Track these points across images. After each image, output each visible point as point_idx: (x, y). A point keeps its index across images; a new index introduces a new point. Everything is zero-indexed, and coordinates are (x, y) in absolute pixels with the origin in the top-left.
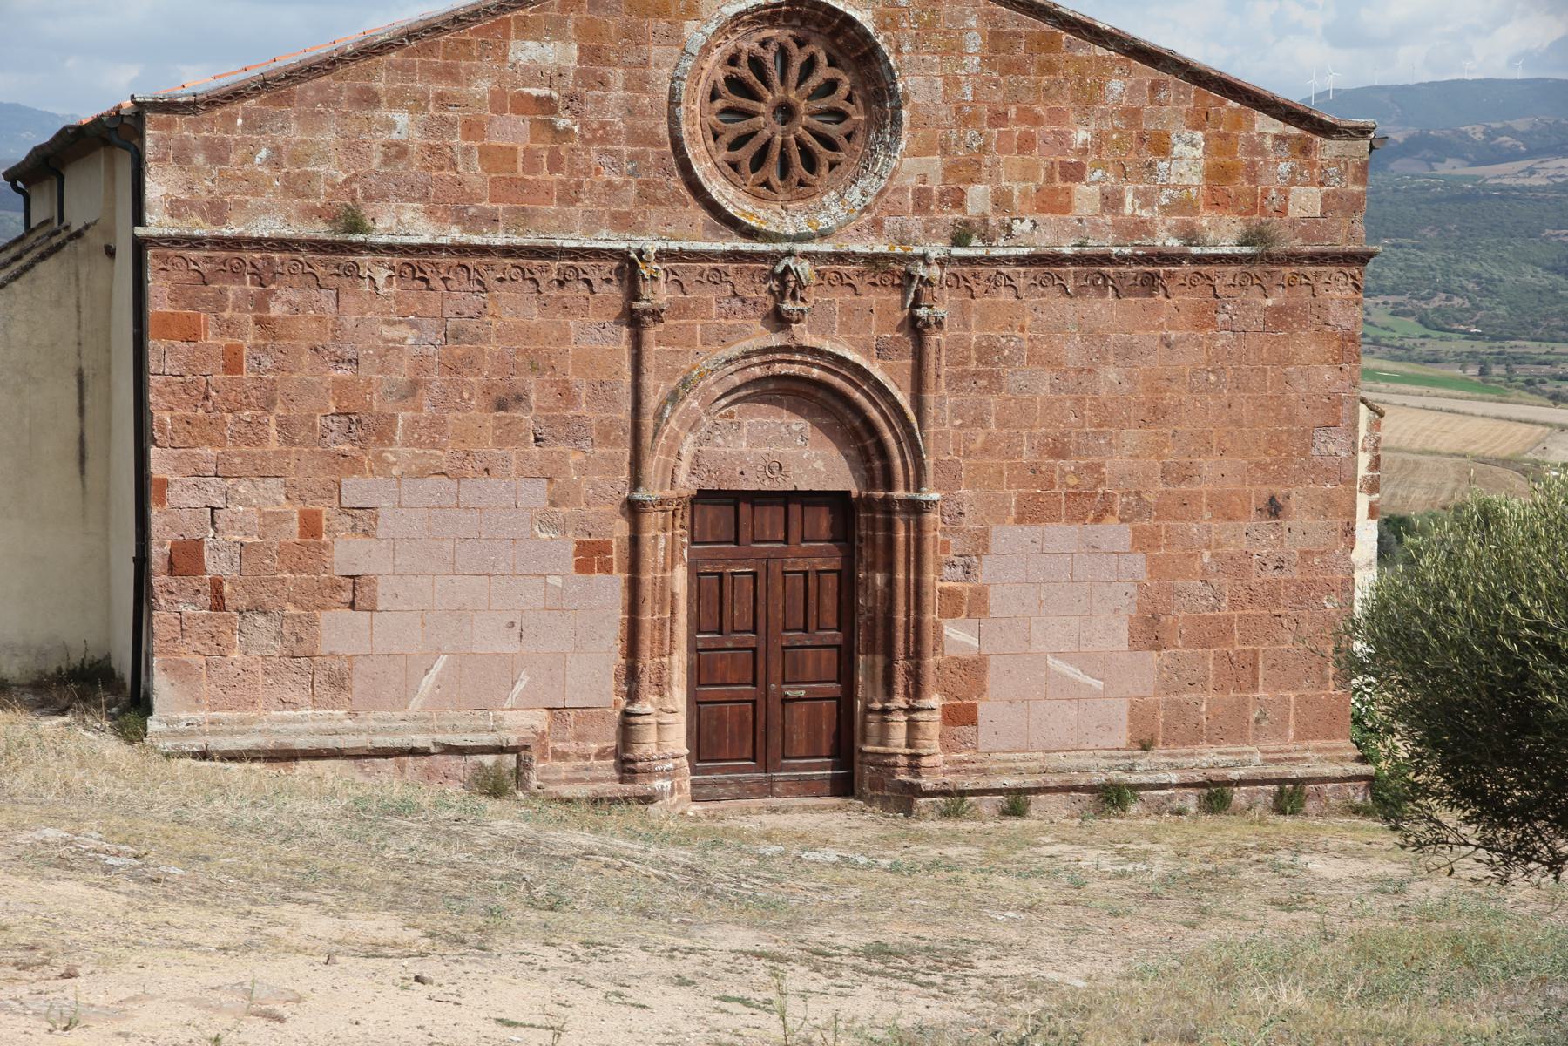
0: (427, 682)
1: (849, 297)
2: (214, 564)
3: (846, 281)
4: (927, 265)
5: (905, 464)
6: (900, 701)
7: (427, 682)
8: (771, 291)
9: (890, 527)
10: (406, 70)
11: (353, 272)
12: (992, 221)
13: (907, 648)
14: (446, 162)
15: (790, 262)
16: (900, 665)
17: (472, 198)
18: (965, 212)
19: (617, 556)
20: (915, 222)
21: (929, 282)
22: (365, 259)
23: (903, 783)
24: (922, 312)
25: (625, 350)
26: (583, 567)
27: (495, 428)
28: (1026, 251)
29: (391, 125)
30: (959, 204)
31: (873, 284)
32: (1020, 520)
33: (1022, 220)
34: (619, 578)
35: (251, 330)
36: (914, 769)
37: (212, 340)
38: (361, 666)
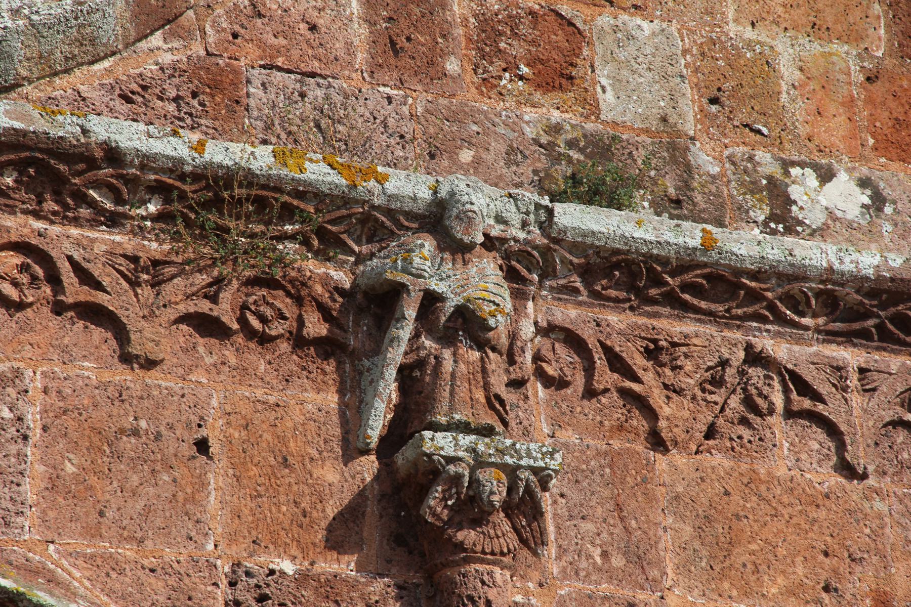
1: (89, 360)
3: (74, 290)
4: (456, 248)
12: (705, 159)
18: (593, 110)
20: (387, 102)
21: (468, 325)
24: (440, 443)
30: (559, 73)
31: (207, 326)
33: (826, 176)
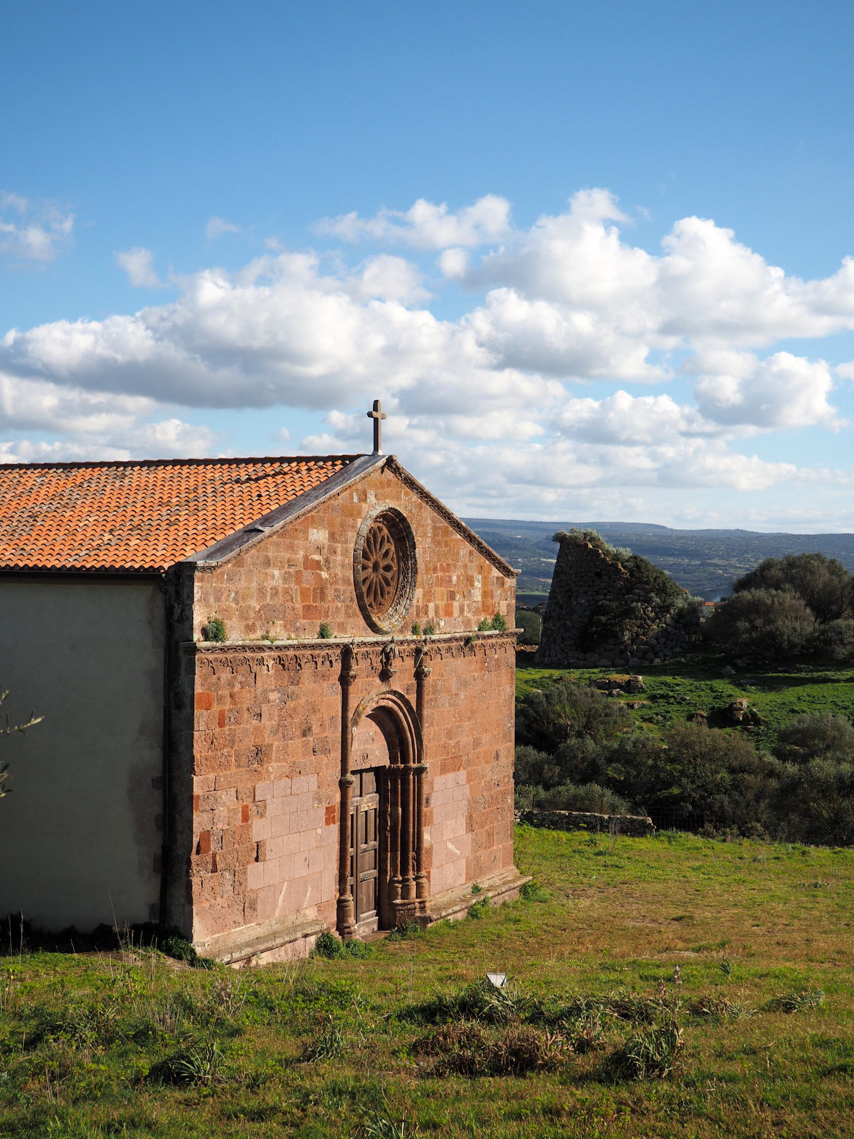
0: (281, 898)
2: (214, 846)
5: (413, 748)
6: (411, 875)
7: (281, 898)
8: (381, 661)
9: (405, 783)
10: (277, 544)
11: (261, 661)
13: (414, 846)
14: (289, 598)
15: (392, 645)
16: (411, 854)
17: (297, 617)
19: (337, 814)
22: (265, 655)
23: (420, 918)
25: (339, 698)
26: (328, 822)
27: (303, 747)
28: (448, 636)
29: (273, 577)
32: (441, 774)
34: (338, 824)
35: (229, 699)
36: (423, 909)
37: (216, 708)
38: (261, 895)
